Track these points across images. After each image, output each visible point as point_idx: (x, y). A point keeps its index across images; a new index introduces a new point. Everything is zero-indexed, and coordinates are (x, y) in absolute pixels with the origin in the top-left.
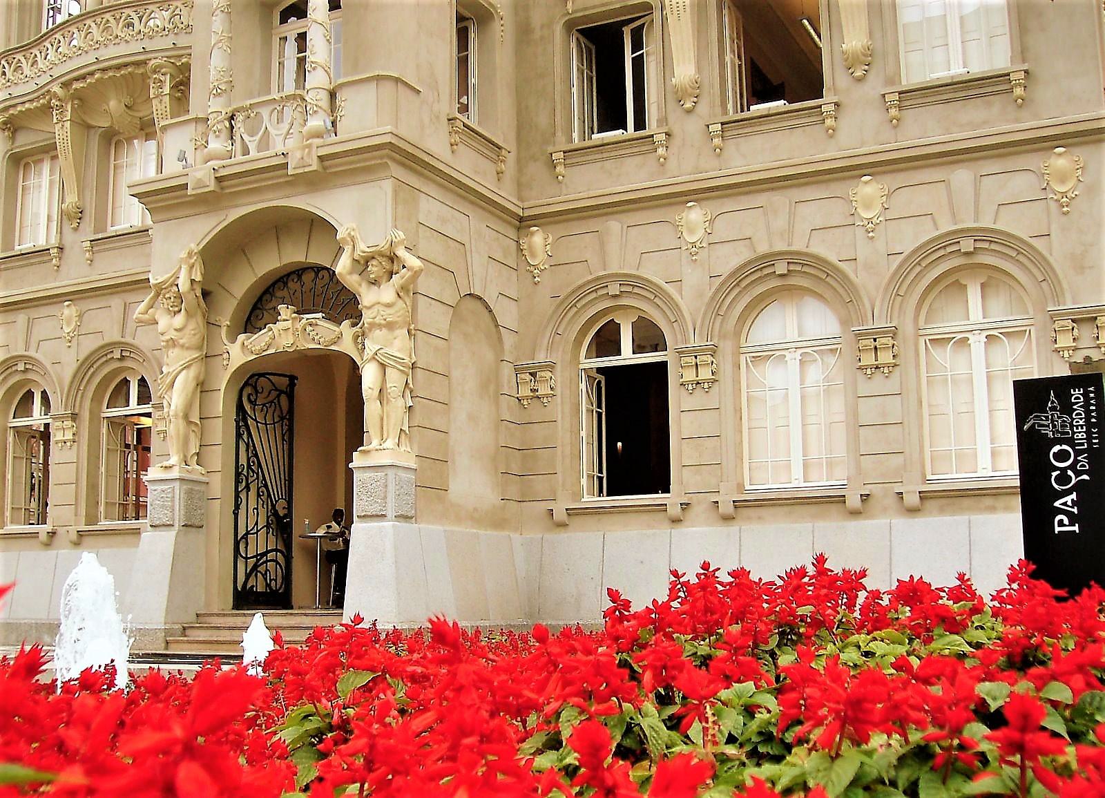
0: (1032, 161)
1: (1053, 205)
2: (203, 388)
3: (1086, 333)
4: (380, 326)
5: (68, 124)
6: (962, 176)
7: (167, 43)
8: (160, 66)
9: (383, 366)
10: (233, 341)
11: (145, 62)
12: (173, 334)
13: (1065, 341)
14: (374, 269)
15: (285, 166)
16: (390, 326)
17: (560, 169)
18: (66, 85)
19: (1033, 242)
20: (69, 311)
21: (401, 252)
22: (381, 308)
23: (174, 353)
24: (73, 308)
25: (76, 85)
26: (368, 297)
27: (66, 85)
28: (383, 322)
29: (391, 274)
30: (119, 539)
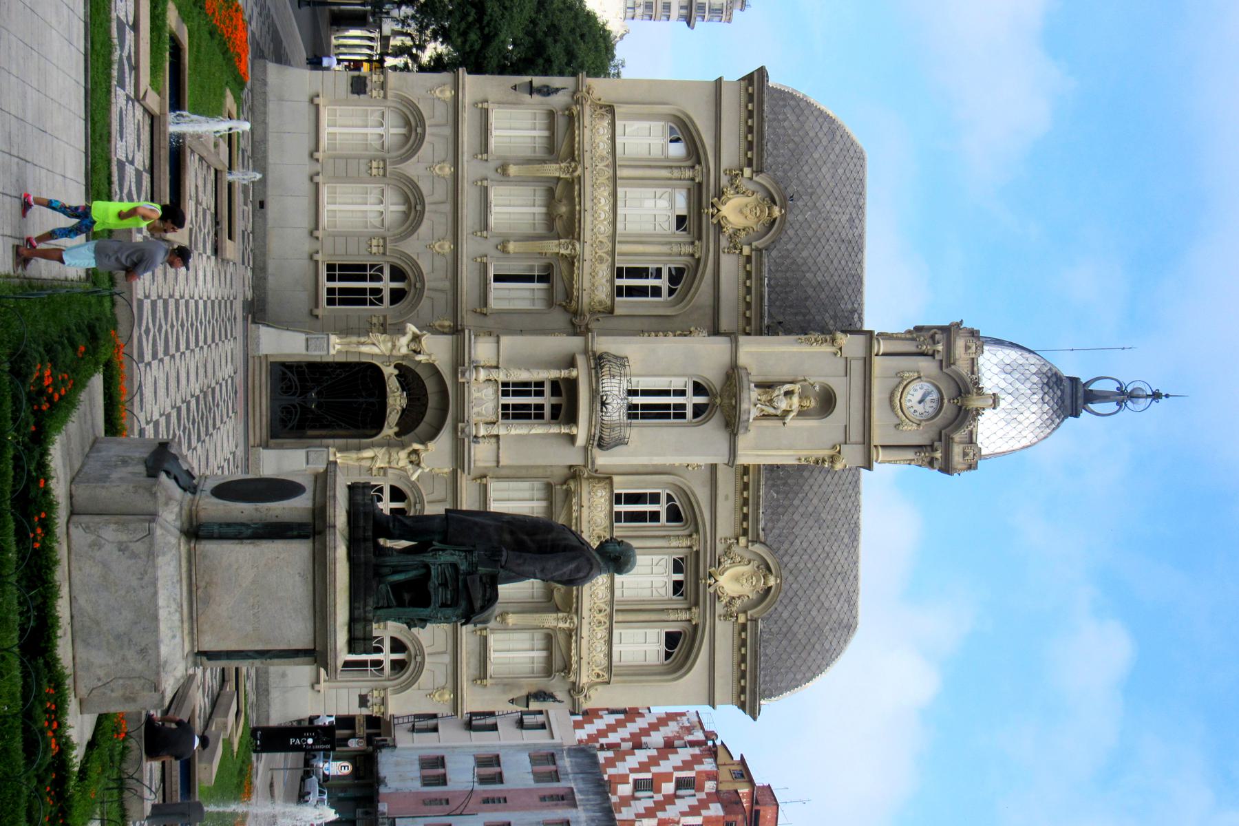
0: (450, 685)
1: (430, 692)
2: (373, 355)
3: (378, 700)
4: (390, 458)
5: (557, 175)
6: (447, 659)
7: (586, 257)
8: (575, 250)
9: (373, 458)
10: (396, 367)
11: (579, 239)
13: (375, 693)
14: (414, 457)
15: (464, 422)
16: (389, 462)
17: (479, 481)
18: (579, 177)
19: (417, 684)
20: (448, 170)
21: (419, 471)
23: (389, 345)
24: (449, 172)
25: (577, 187)
26: (403, 454)
27: (579, 177)
29: (411, 462)
30: (313, 211)
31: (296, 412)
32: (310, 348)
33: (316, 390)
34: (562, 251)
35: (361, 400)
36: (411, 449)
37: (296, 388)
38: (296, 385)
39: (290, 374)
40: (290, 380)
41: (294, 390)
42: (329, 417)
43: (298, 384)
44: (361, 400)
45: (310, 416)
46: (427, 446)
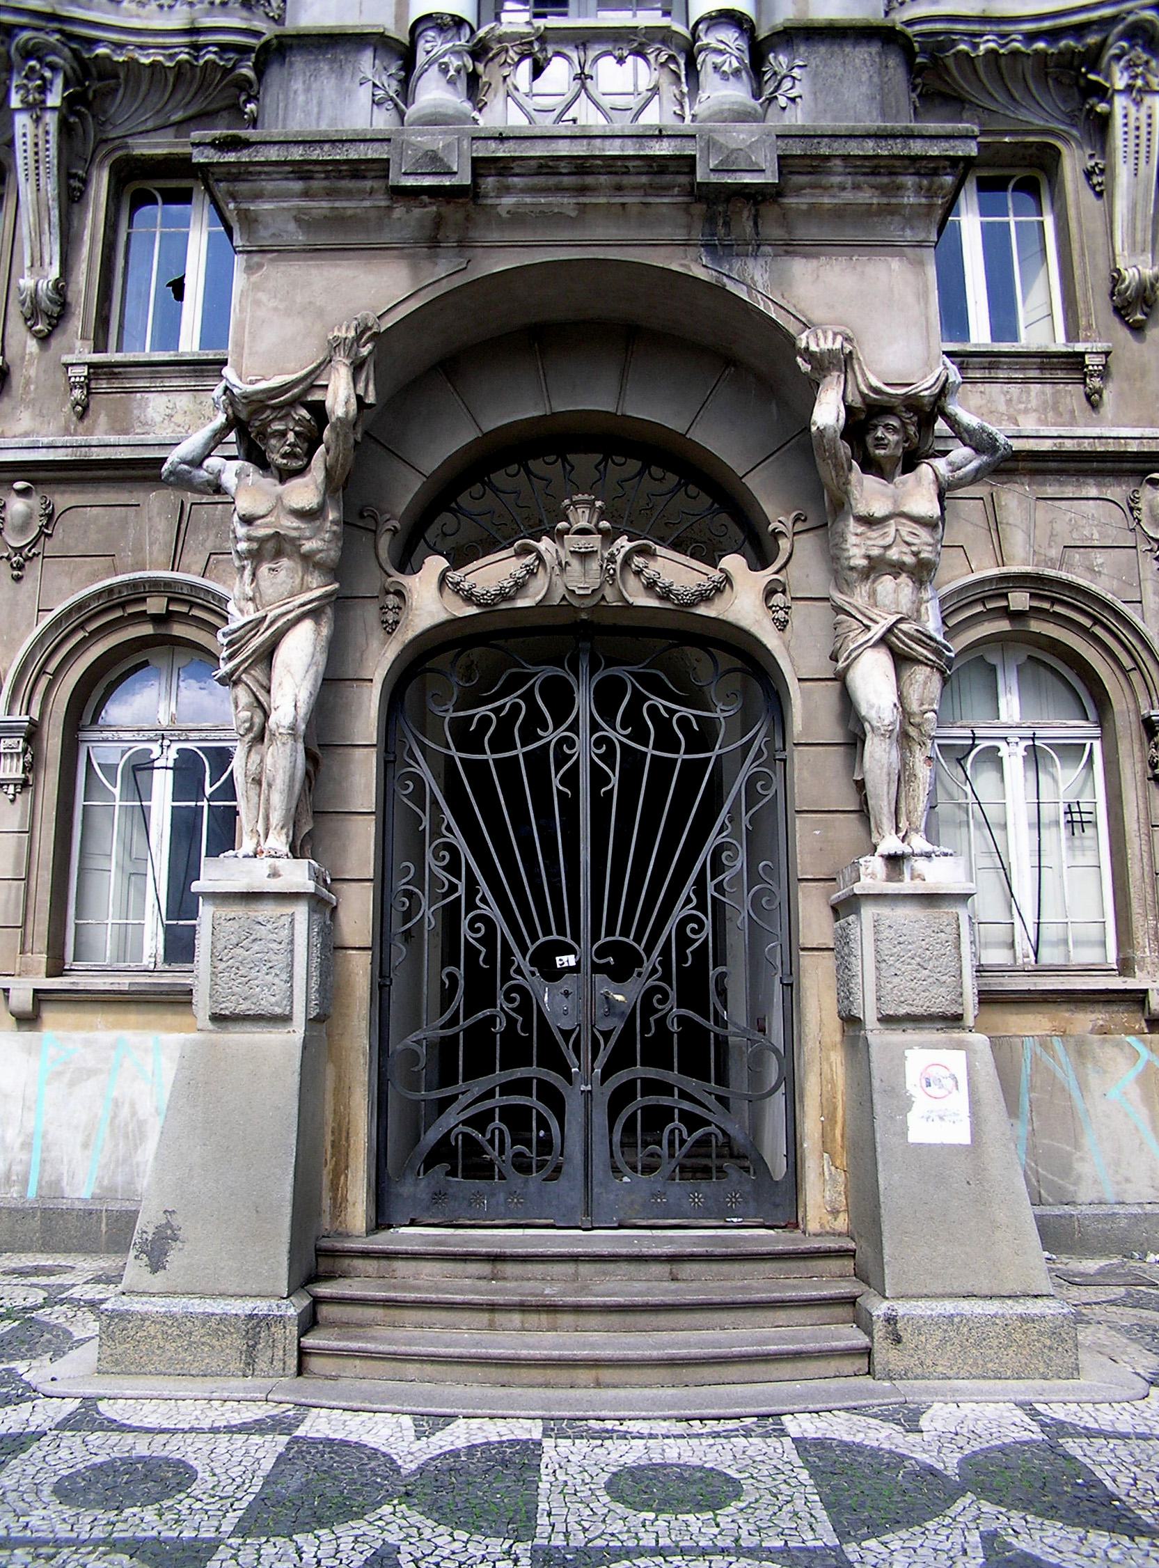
4: (897, 569)
12: (289, 525)
14: (888, 438)
22: (906, 528)
28: (909, 559)
31: (652, 1087)
32: (269, 1003)
33: (533, 981)
34: (54, 99)
35: (584, 750)
36: (844, 448)
37: (521, 1087)
38: (507, 1089)
39: (451, 1119)
40: (480, 1121)
41: (532, 1101)
42: (678, 914)
43: (500, 1076)
44: (584, 750)
45: (673, 1011)
46: (823, 364)
